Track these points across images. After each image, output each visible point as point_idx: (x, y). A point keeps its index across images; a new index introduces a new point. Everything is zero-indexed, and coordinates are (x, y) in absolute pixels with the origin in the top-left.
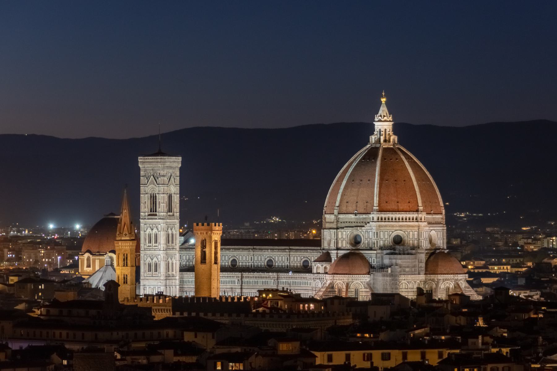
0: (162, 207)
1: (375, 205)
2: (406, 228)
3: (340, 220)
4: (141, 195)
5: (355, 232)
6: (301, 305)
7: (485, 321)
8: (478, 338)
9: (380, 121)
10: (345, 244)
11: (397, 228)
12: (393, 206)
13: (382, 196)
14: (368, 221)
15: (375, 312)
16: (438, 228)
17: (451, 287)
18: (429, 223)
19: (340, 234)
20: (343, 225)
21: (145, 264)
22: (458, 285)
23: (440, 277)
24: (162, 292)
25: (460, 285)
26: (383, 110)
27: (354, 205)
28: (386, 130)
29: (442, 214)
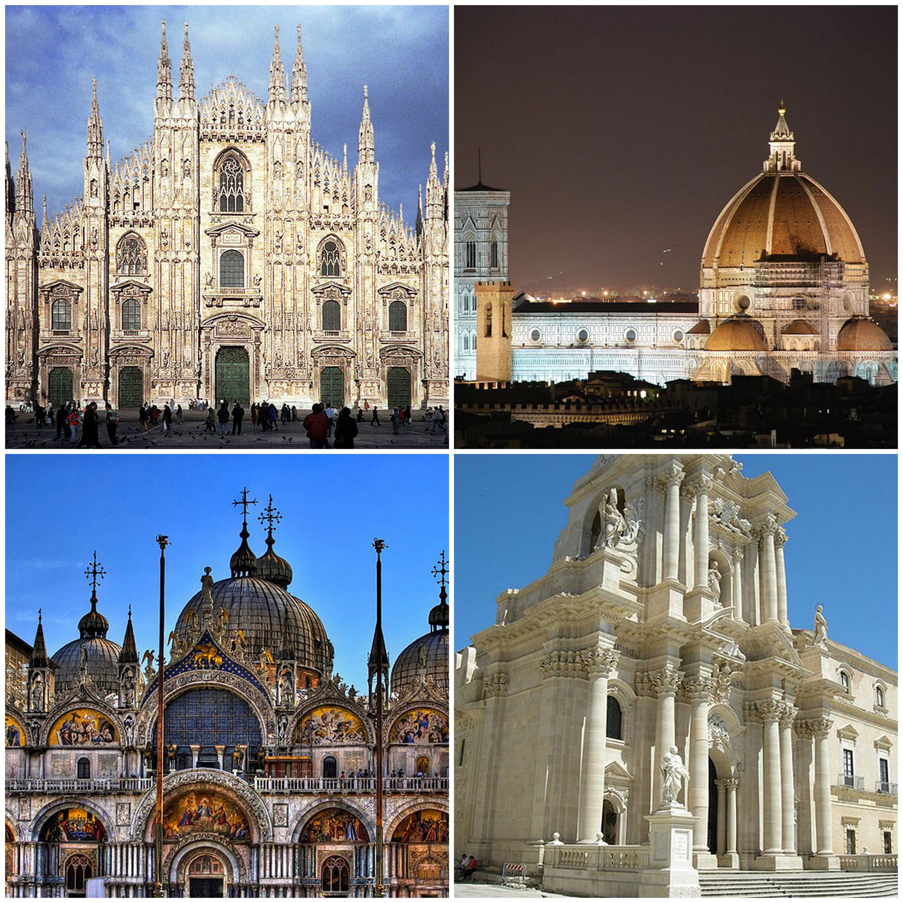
0: (483, 261)
3: (721, 277)
5: (742, 294)
6: (635, 393)
7: (858, 414)
8: (770, 433)
9: (776, 140)
10: (728, 309)
20: (725, 283)
22: (884, 365)
23: (857, 354)
26: (781, 126)
27: (740, 256)
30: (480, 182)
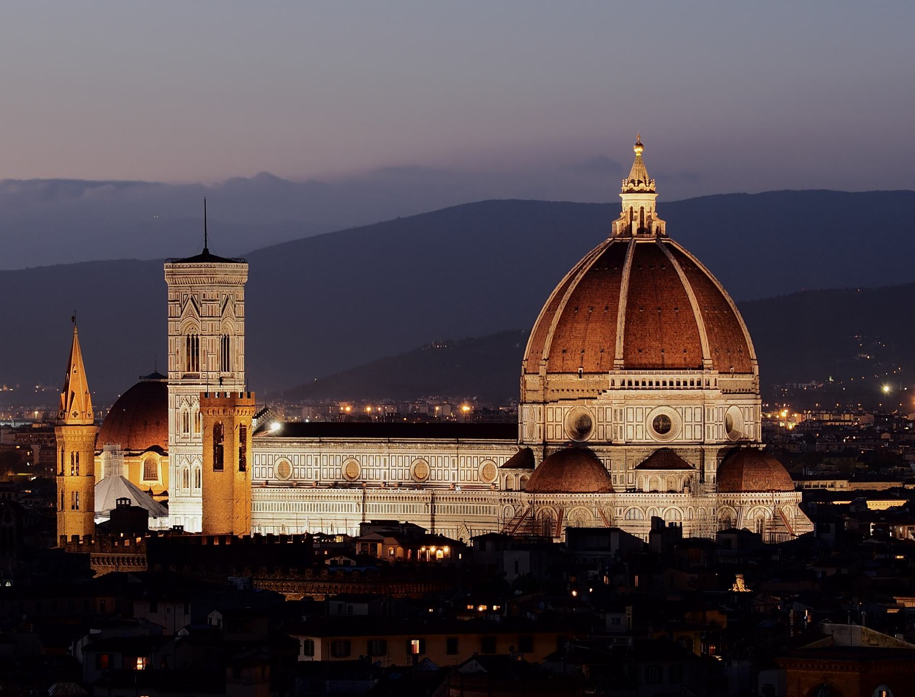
0: (210, 362)
1: (617, 356)
2: (678, 402)
3: (550, 386)
4: (170, 338)
8: (624, 611)
9: (631, 191)
11: (662, 402)
12: (654, 359)
13: (631, 338)
14: (605, 387)
15: (517, 563)
16: (745, 402)
17: (767, 516)
18: (725, 392)
19: (550, 412)
20: (557, 396)
21: (177, 472)
22: (782, 513)
23: (744, 497)
24: (182, 527)
25: (786, 513)
28: (642, 208)
29: (752, 373)
30: (206, 250)
